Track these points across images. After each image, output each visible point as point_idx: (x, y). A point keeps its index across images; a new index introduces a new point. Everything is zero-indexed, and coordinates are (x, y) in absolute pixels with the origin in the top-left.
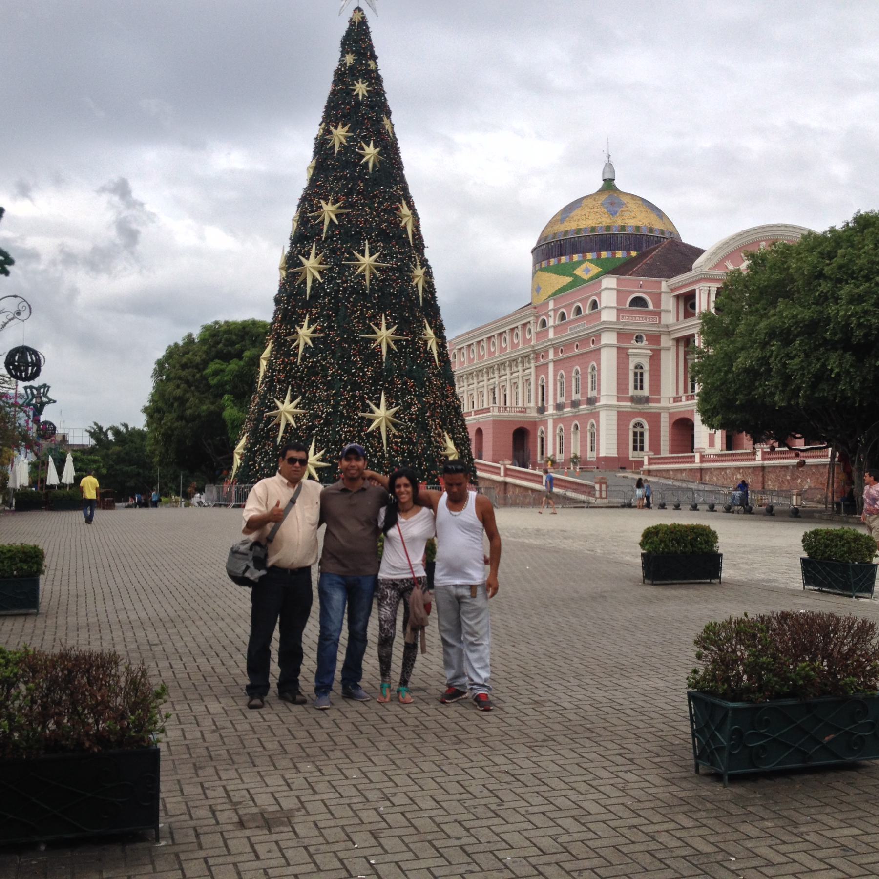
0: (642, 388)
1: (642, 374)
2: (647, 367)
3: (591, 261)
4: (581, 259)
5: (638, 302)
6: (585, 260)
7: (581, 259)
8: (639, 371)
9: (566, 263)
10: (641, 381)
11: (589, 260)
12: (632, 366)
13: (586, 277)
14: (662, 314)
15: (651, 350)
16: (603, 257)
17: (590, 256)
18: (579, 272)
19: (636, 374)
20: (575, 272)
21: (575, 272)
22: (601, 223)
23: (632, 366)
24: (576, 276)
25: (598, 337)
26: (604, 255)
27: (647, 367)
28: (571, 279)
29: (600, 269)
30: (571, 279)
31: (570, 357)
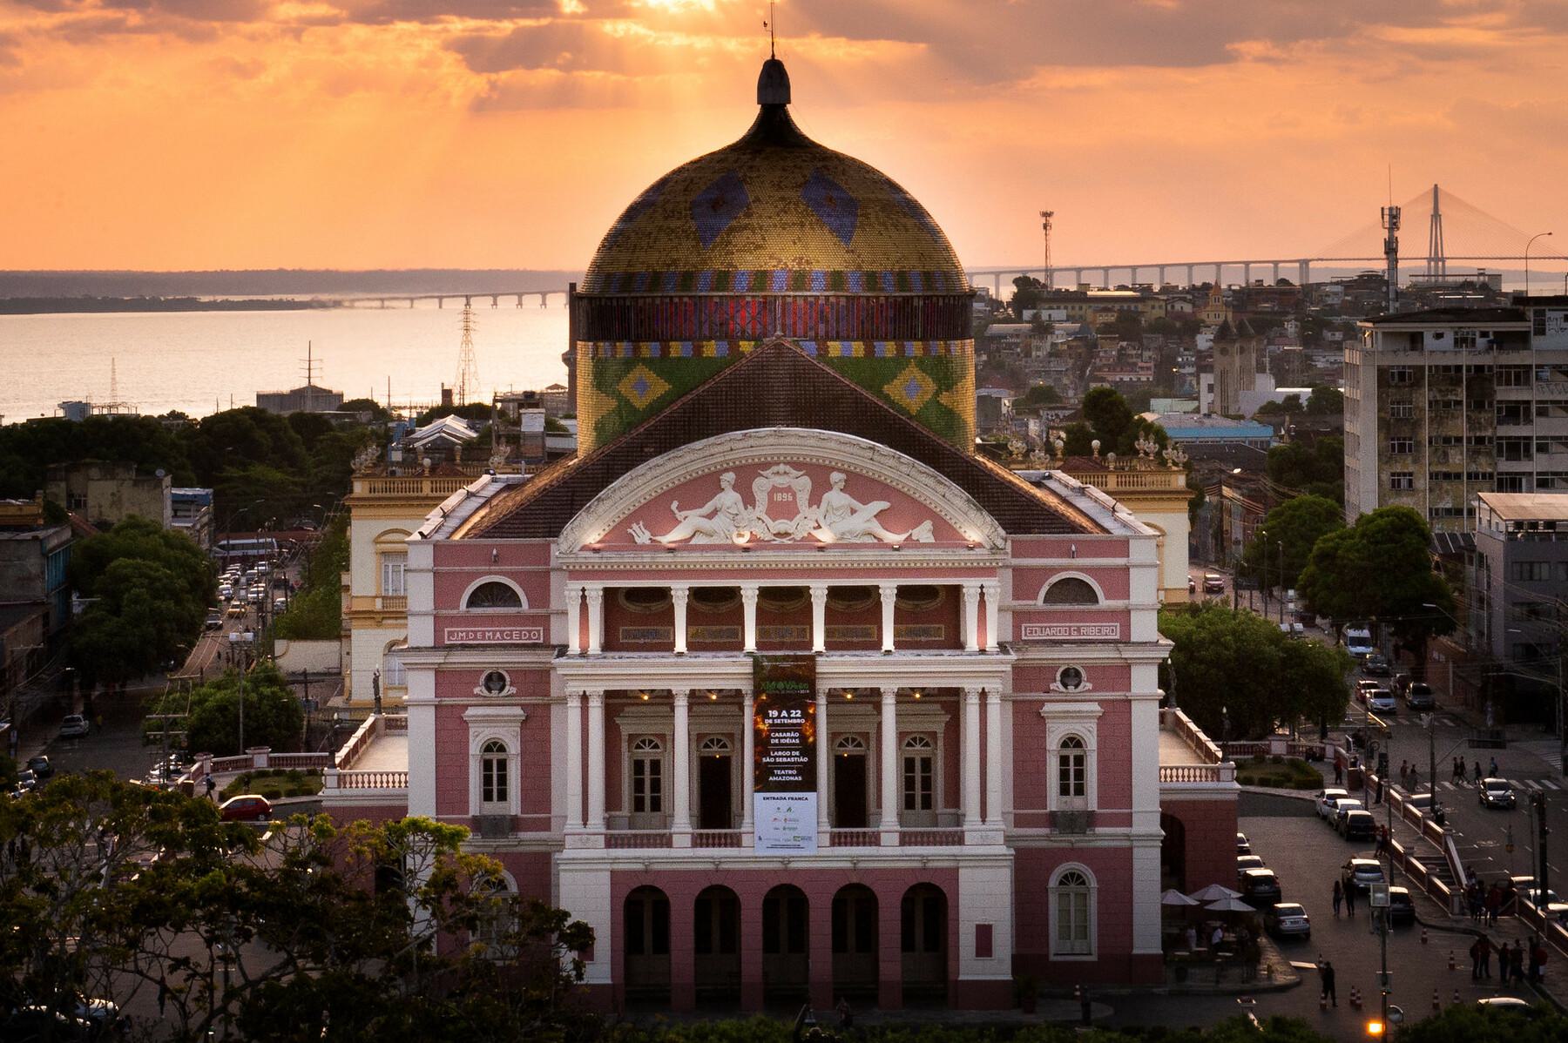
0: (503, 796)
1: (502, 765)
2: (514, 747)
3: (649, 363)
5: (492, 594)
8: (495, 757)
10: (503, 780)
11: (644, 361)
12: (475, 749)
14: (553, 619)
15: (523, 706)
16: (673, 354)
17: (649, 349)
19: (487, 765)
22: (674, 262)
23: (475, 749)
26: (677, 349)
27: (514, 747)
29: (668, 387)
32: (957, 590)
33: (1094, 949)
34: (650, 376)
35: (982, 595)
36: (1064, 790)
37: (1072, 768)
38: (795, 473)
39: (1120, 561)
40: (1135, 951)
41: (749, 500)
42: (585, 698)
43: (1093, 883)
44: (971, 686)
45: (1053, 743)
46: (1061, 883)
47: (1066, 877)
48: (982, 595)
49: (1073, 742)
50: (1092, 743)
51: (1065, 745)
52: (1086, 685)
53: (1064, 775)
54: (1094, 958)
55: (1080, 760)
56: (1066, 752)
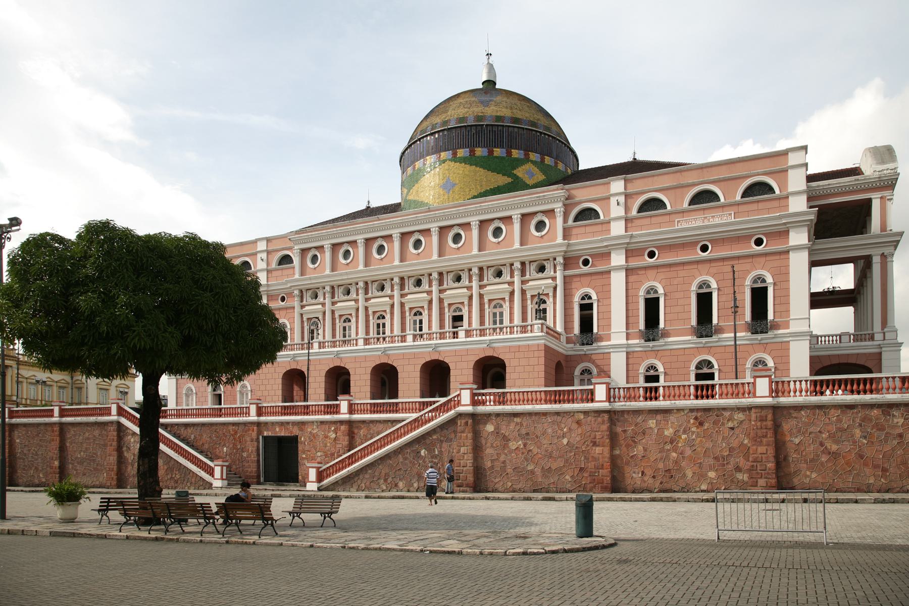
4: (522, 157)
6: (527, 159)
7: (522, 157)
9: (502, 158)
11: (532, 162)
13: (530, 182)
17: (534, 156)
18: (520, 172)
20: (515, 172)
21: (515, 172)
24: (516, 177)
25: (784, 234)
26: (548, 160)
28: (510, 180)
30: (510, 180)
31: (683, 264)
34: (535, 170)
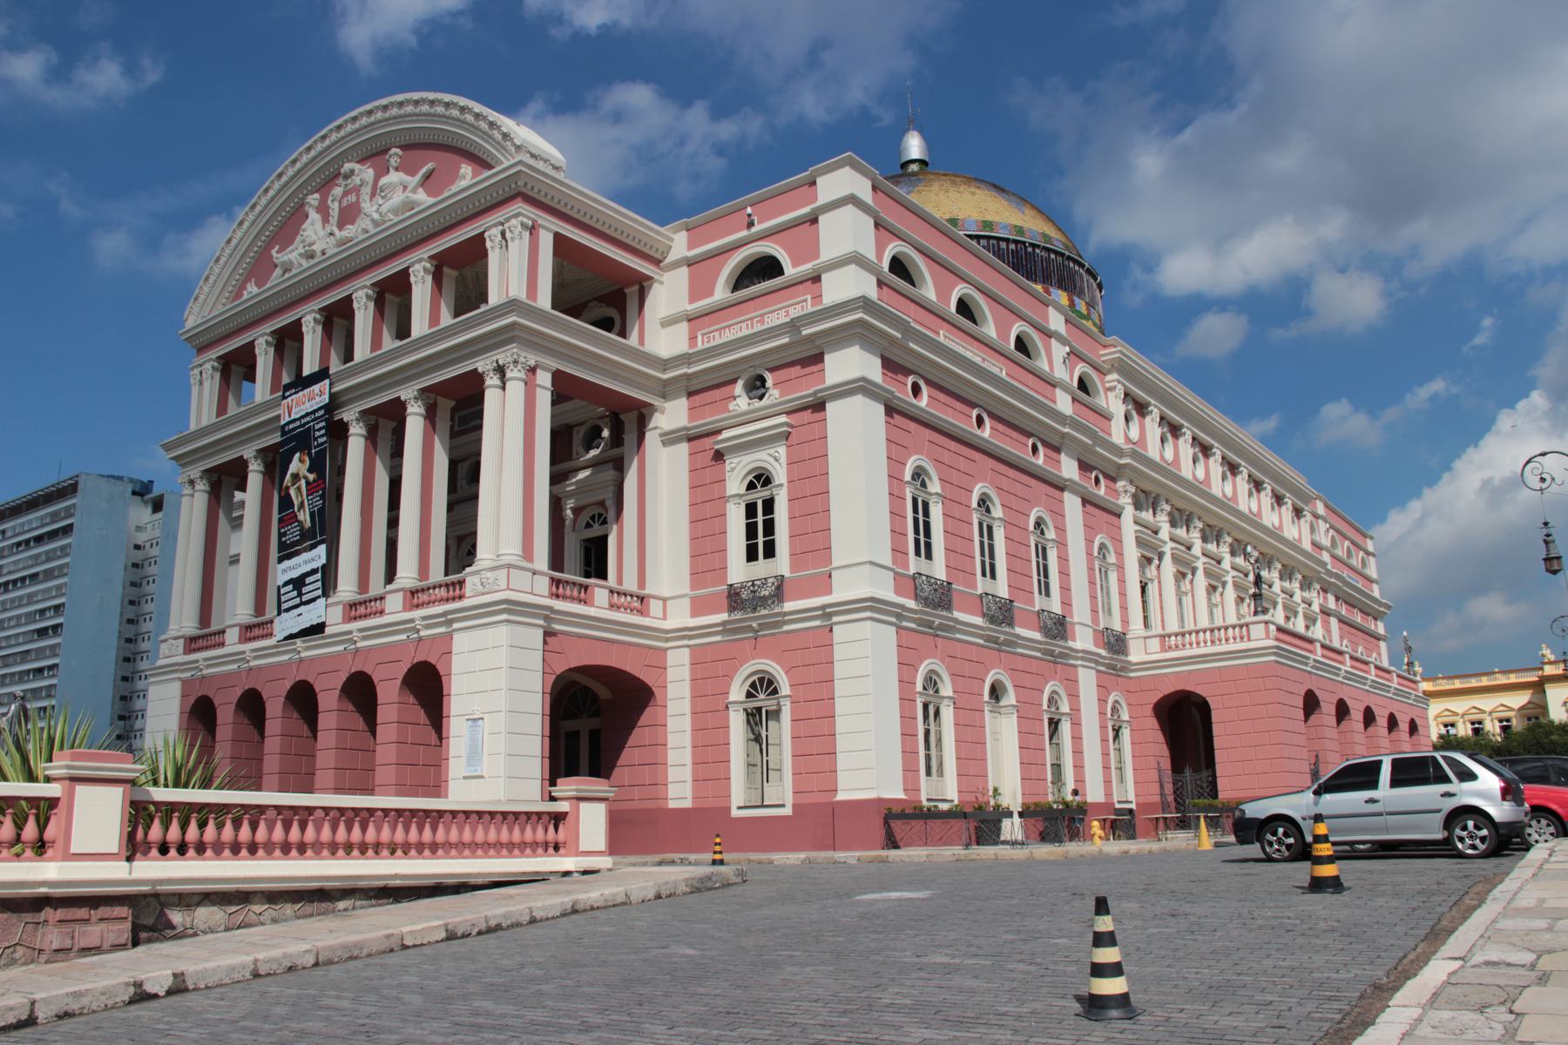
32: (480, 239)
33: (789, 800)
35: (503, 234)
36: (752, 555)
37: (760, 519)
38: (357, 167)
39: (807, 210)
40: (841, 796)
41: (326, 220)
42: (192, 482)
43: (785, 689)
44: (483, 364)
45: (735, 484)
46: (749, 695)
47: (753, 685)
48: (503, 234)
49: (761, 479)
50: (780, 475)
51: (751, 486)
52: (773, 395)
53: (751, 531)
54: (787, 811)
55: (769, 505)
56: (752, 496)
